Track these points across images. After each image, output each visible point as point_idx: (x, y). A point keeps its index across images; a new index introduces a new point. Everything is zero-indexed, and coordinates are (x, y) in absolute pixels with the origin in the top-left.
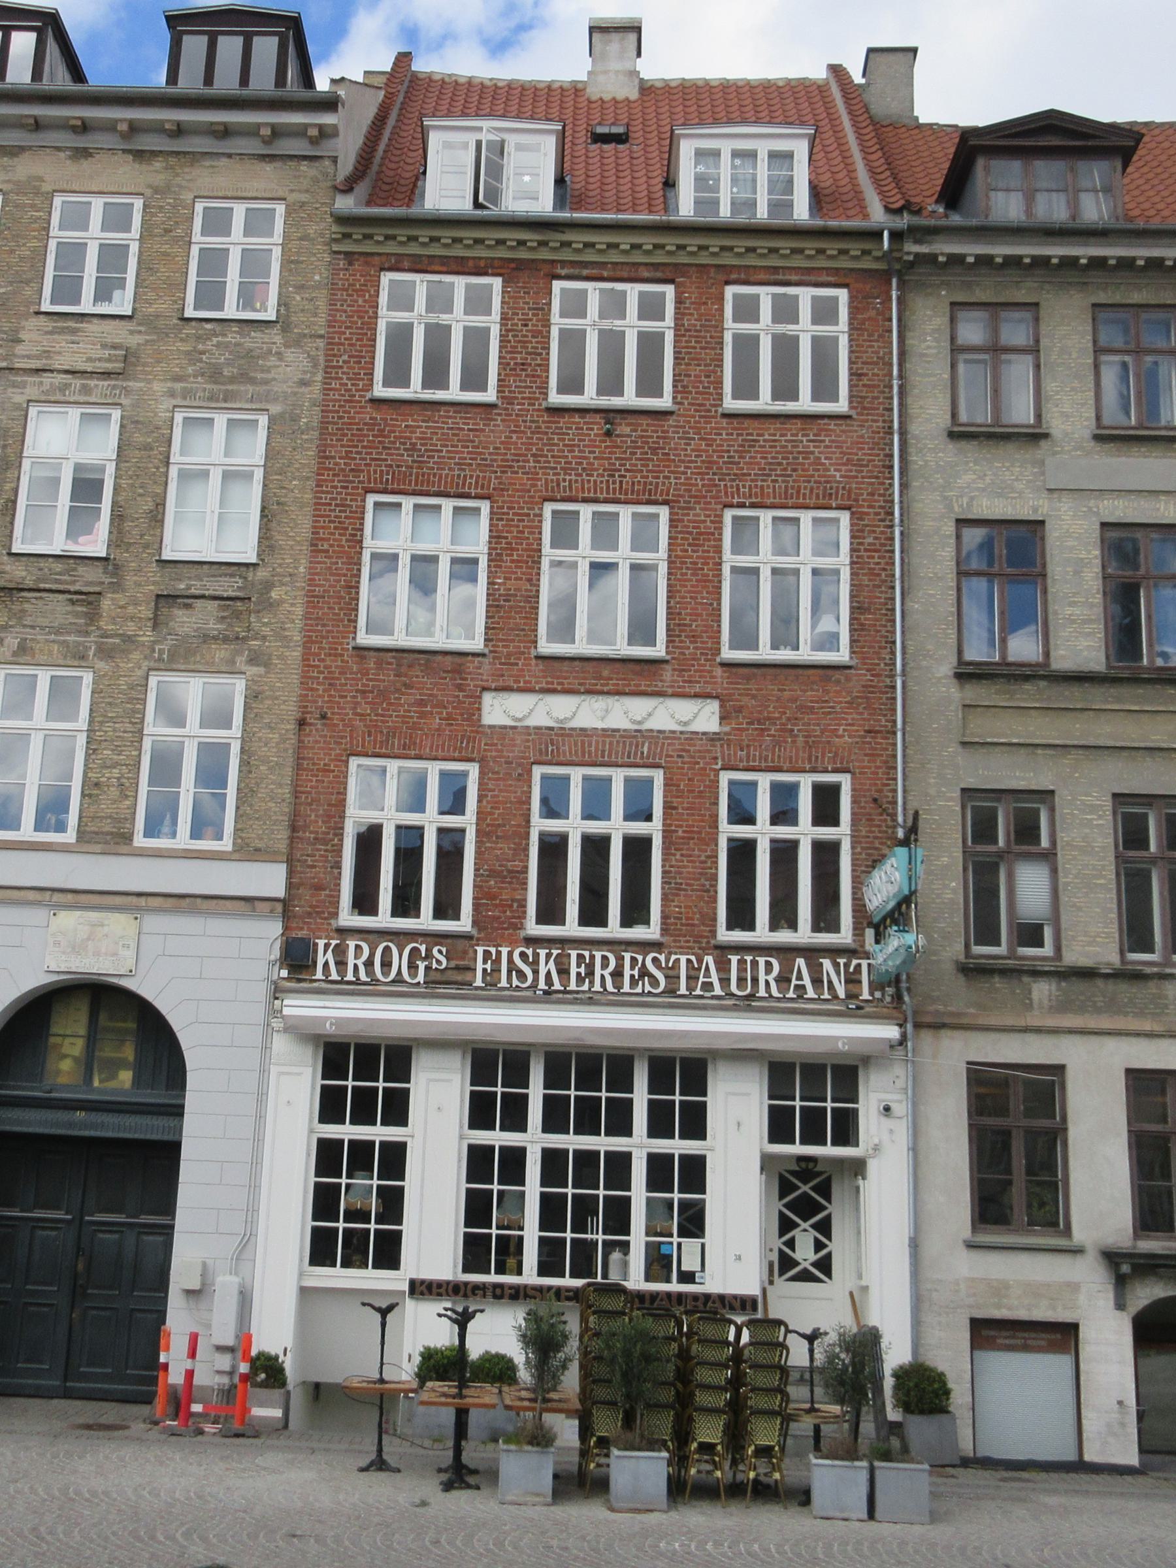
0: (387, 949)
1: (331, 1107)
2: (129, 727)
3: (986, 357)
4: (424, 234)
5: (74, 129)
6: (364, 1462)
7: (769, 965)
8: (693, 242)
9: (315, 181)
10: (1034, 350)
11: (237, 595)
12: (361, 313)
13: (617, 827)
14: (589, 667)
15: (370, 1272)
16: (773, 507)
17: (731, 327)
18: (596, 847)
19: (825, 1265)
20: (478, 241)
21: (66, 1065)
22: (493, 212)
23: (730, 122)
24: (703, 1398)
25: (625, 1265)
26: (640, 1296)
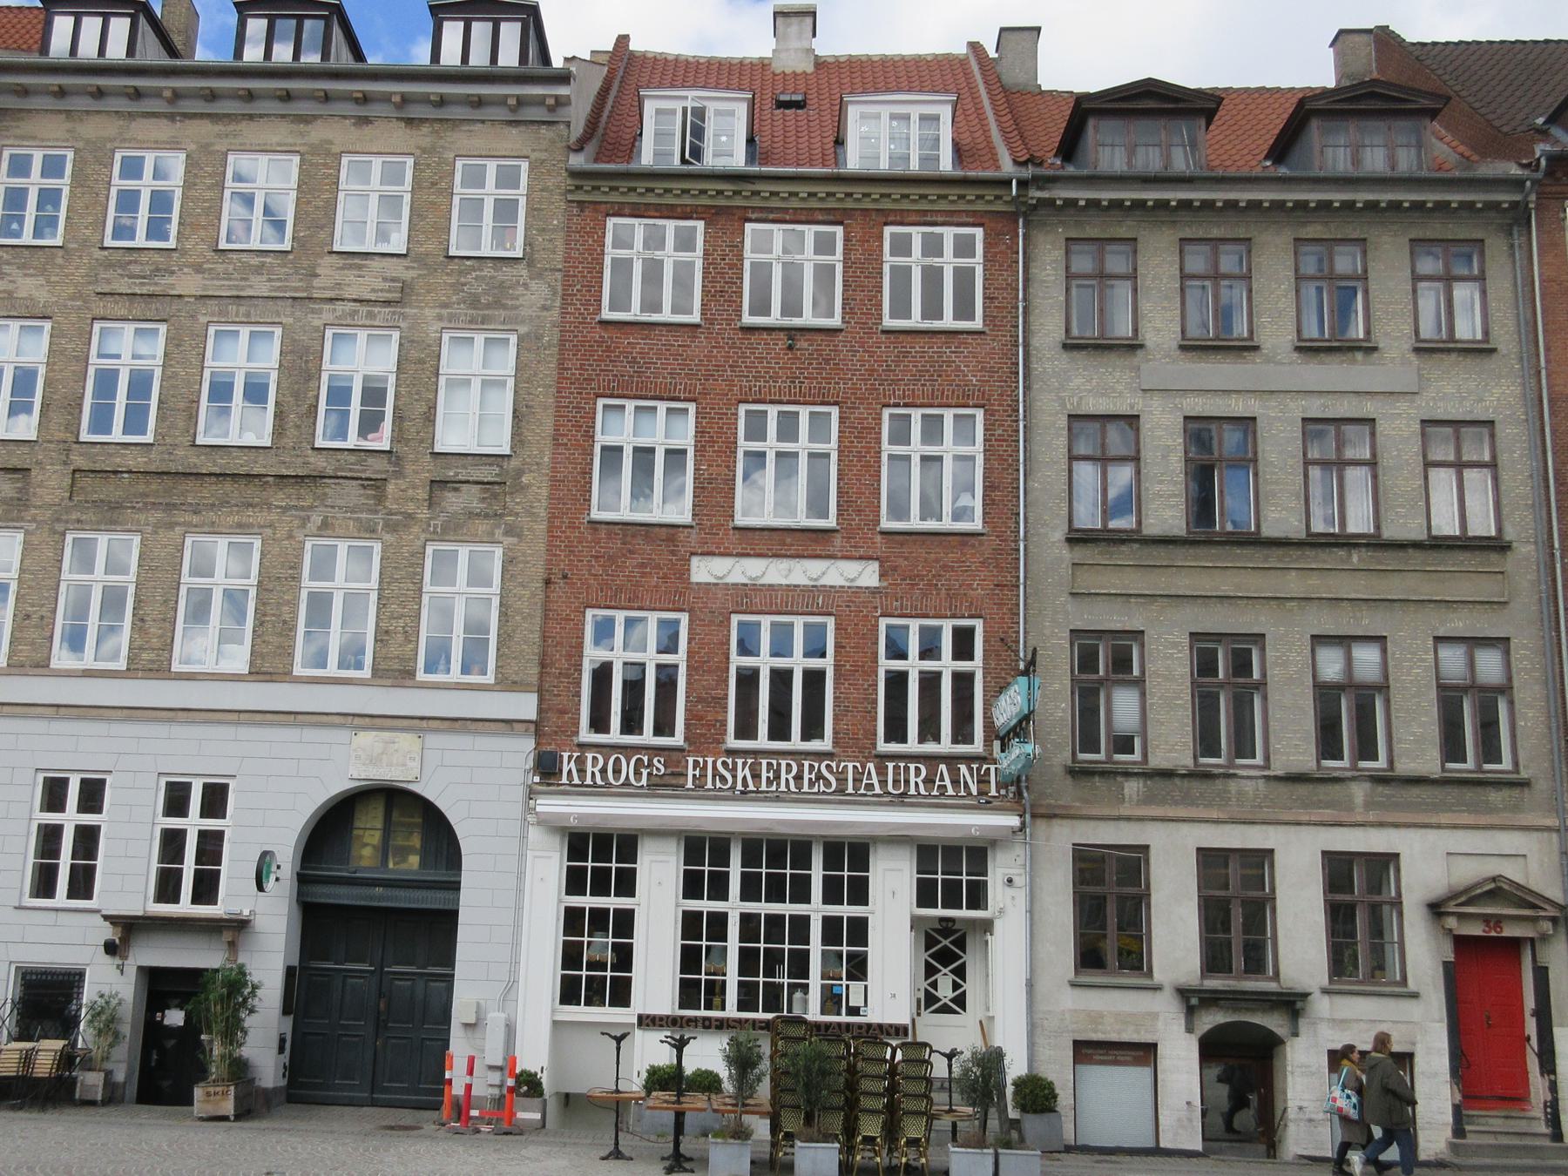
0: (617, 759)
1: (575, 883)
3: (1094, 282)
4: (641, 186)
5: (357, 101)
6: (605, 1153)
7: (917, 769)
8: (858, 190)
9: (553, 142)
10: (1133, 277)
11: (494, 480)
12: (590, 251)
13: (798, 663)
14: (775, 535)
15: (607, 1009)
16: (922, 406)
17: (889, 260)
18: (781, 679)
19: (960, 1001)
20: (685, 191)
21: (367, 852)
22: (696, 167)
23: (888, 90)
24: (866, 1103)
25: (806, 1002)
26: (817, 1026)
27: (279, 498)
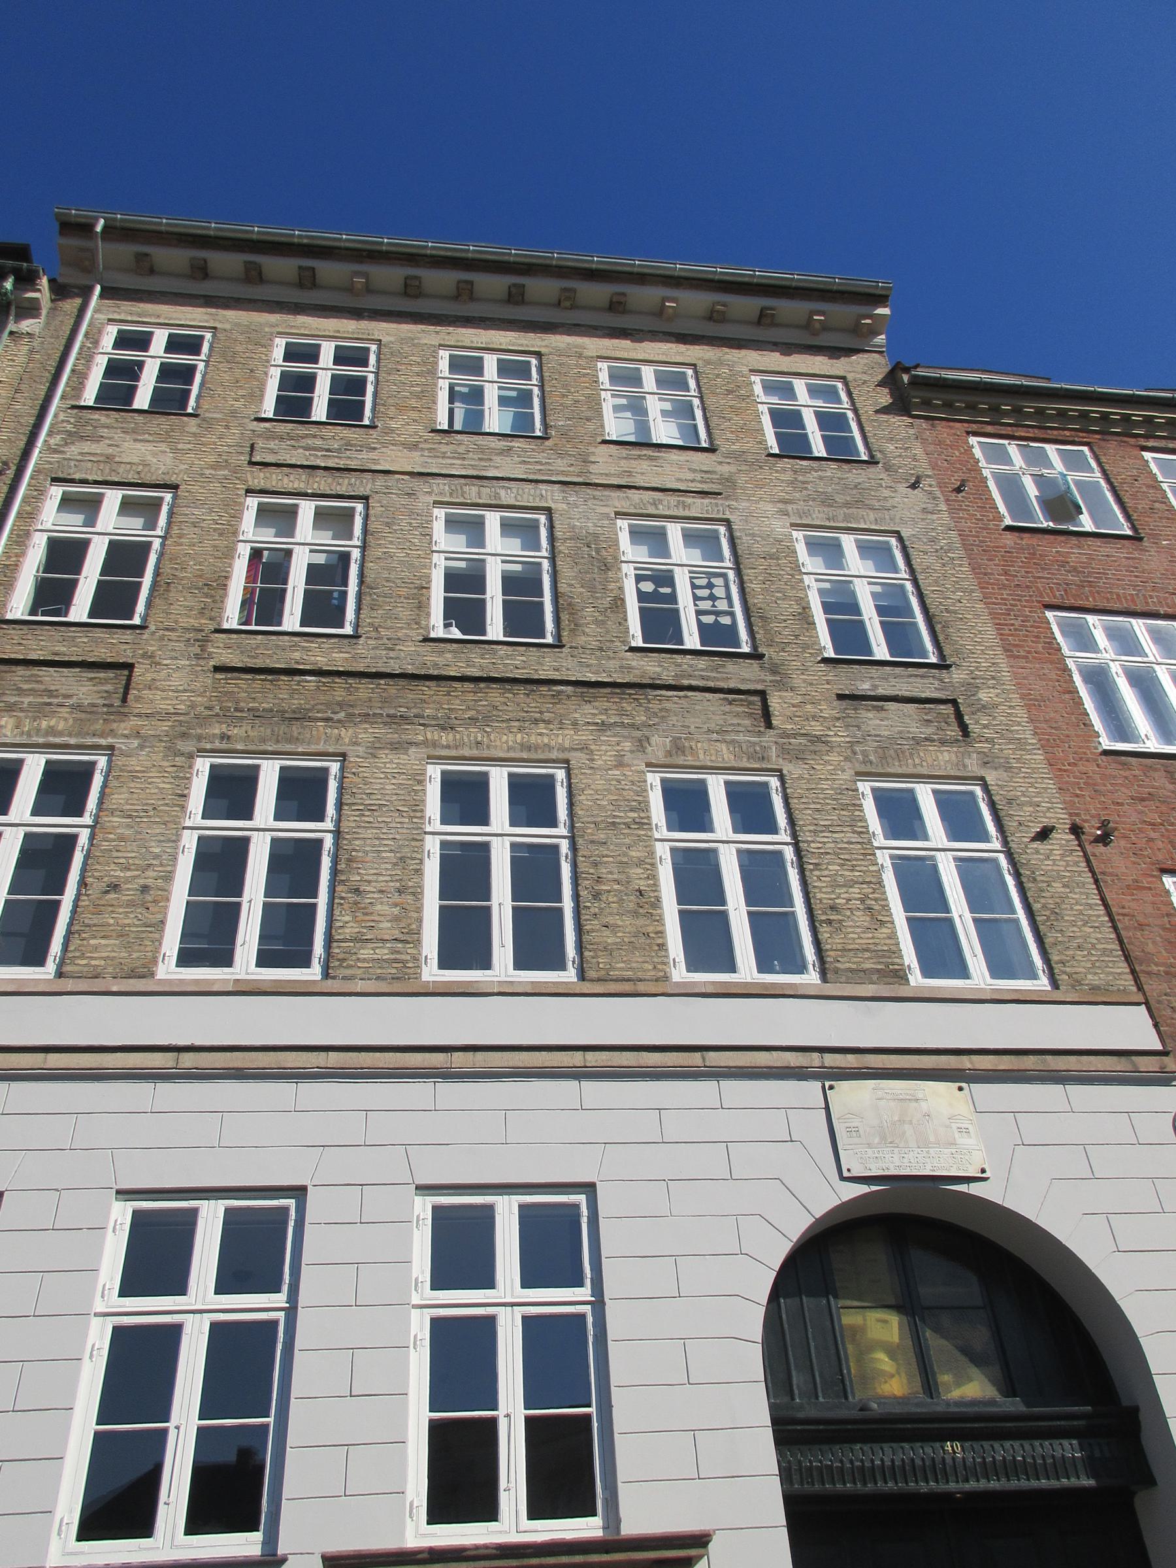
2: (855, 838)
27: (588, 711)
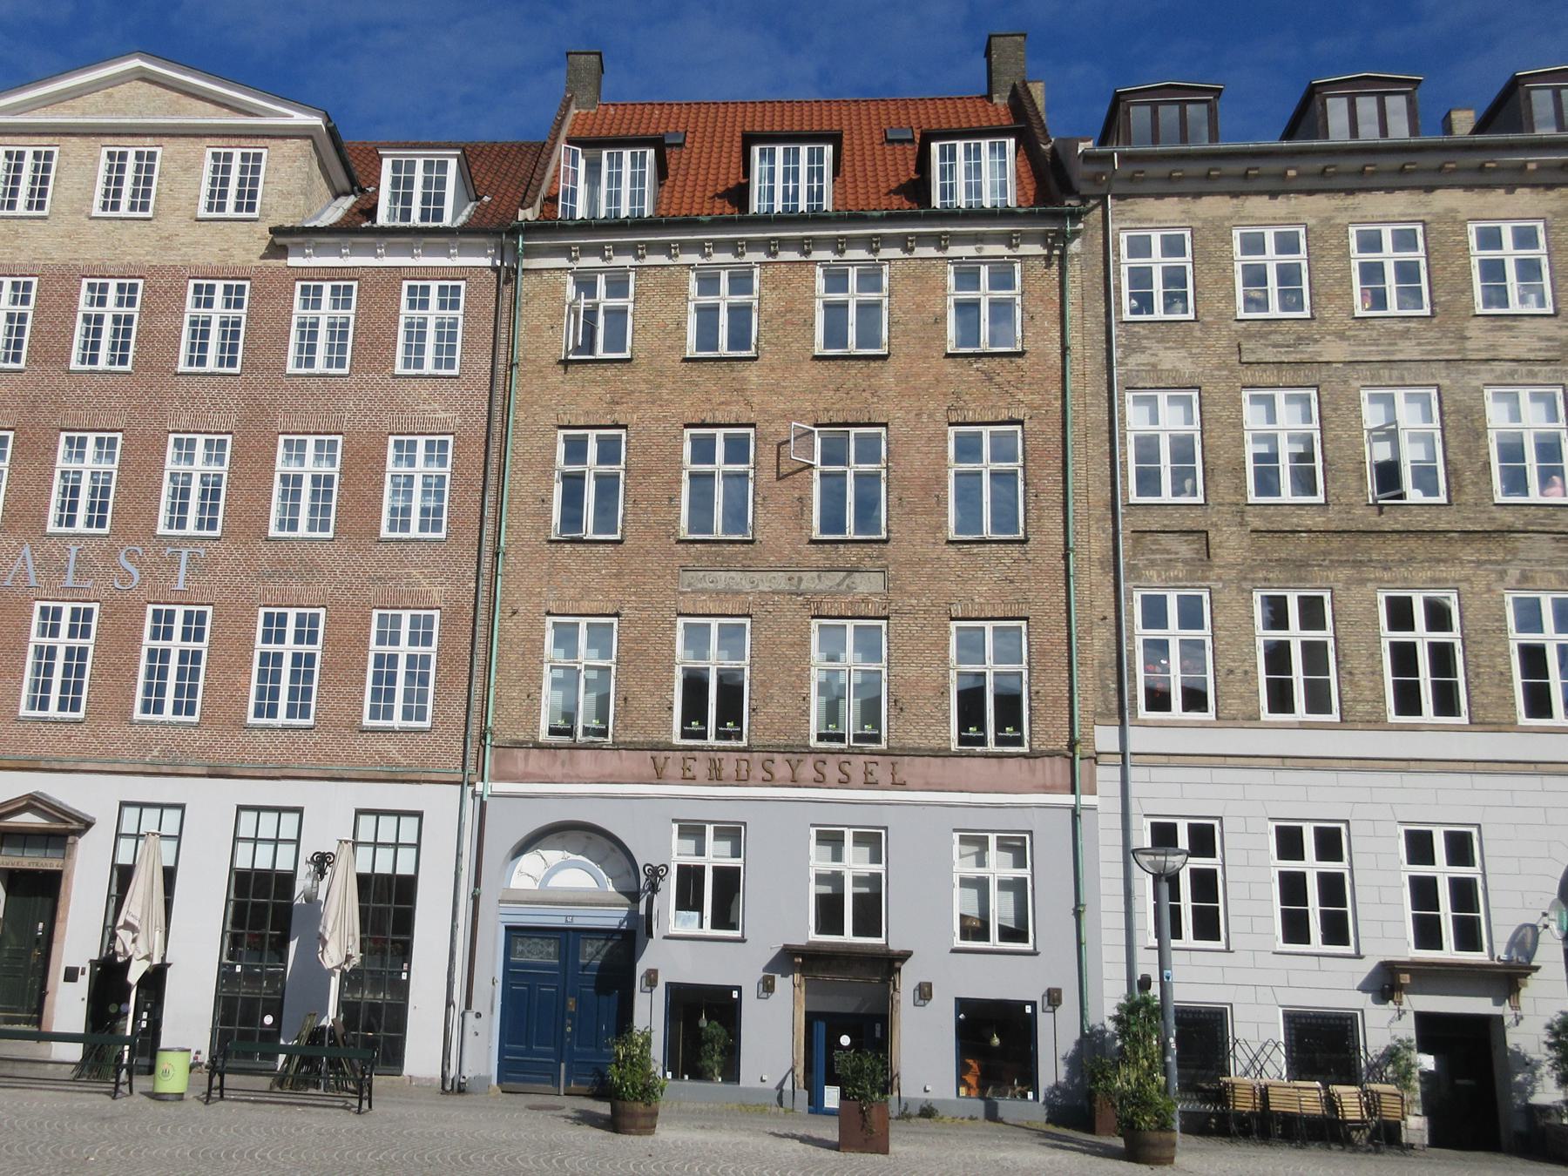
27: (1468, 553)
